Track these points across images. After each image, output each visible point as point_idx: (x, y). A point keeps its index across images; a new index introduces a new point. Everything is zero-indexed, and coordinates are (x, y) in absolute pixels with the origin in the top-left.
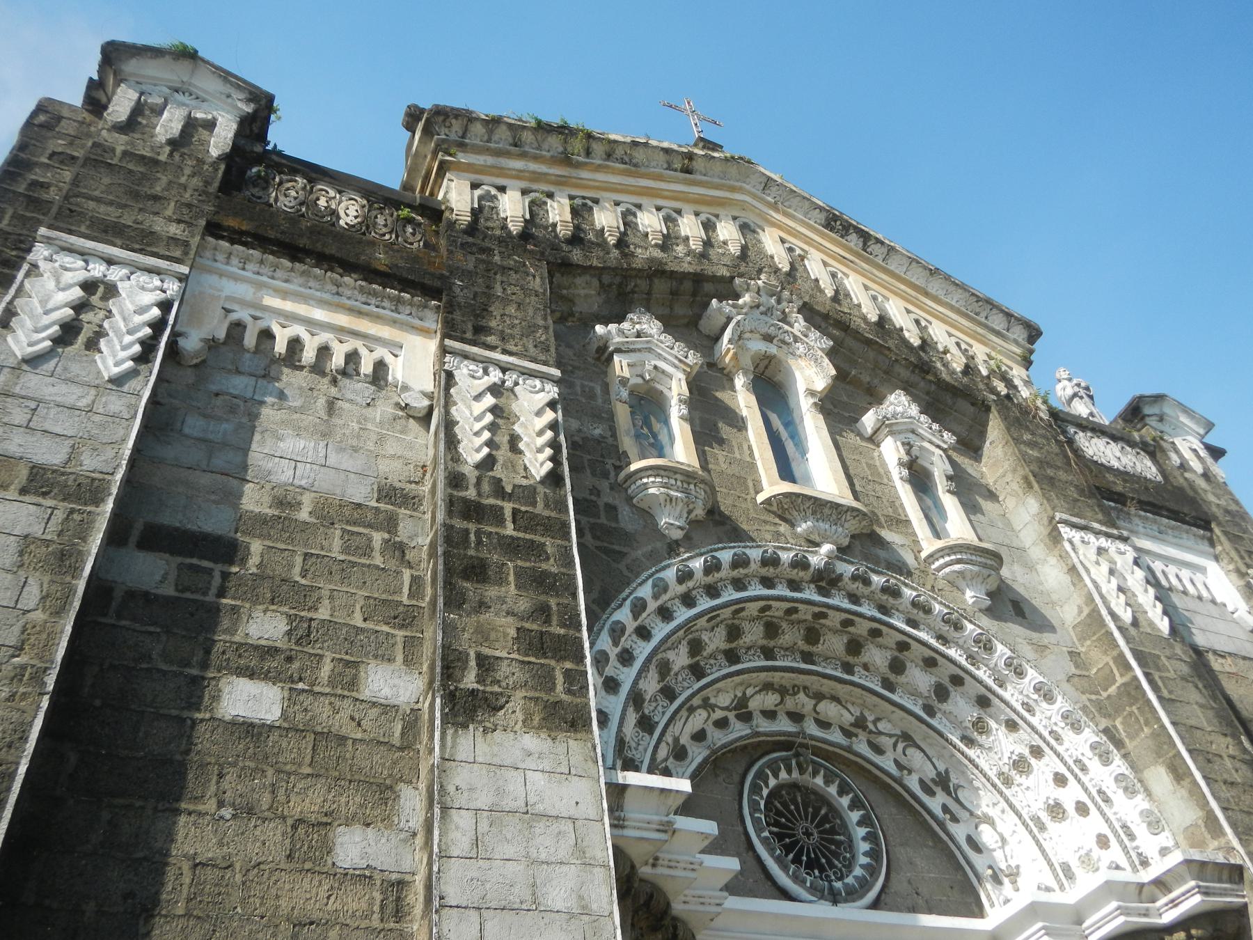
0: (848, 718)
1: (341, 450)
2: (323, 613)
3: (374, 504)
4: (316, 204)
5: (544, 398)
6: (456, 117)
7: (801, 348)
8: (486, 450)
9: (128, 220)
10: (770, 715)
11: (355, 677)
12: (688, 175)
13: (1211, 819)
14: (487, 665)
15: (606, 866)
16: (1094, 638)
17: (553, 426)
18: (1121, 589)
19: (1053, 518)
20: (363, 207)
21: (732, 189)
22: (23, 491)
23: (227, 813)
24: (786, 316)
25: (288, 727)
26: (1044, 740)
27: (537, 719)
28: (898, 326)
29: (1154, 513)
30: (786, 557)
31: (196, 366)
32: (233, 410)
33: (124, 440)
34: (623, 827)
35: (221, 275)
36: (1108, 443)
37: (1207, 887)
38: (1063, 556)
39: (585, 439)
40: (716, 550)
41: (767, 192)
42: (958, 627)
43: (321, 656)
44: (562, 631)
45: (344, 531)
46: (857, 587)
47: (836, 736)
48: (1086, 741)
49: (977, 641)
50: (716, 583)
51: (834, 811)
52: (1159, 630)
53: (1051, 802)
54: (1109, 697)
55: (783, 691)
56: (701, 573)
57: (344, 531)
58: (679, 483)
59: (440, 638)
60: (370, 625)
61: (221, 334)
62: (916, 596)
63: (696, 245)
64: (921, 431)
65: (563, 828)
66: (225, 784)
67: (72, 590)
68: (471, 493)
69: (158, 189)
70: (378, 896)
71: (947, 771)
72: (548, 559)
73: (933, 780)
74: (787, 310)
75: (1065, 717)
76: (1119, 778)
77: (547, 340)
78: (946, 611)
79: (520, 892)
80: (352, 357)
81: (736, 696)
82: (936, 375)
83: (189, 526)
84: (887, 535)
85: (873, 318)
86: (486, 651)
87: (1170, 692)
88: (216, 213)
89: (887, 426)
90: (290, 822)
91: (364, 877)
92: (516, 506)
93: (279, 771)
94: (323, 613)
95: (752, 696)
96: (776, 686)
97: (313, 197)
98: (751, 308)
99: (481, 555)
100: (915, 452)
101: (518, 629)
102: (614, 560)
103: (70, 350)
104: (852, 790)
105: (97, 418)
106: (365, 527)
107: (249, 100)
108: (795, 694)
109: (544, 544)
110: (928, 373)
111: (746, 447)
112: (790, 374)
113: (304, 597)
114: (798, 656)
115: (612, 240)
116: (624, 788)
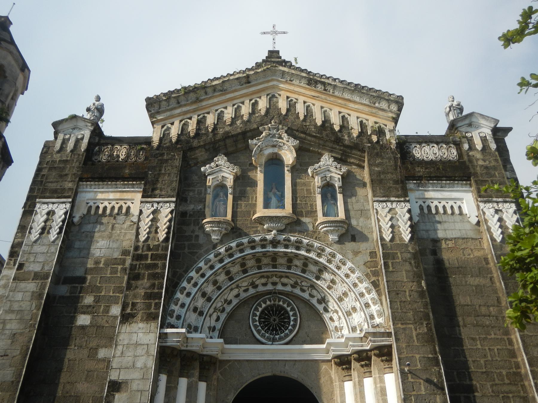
0: (292, 282)
1: (113, 241)
2: (103, 294)
3: (120, 257)
5: (169, 210)
6: (155, 103)
8: (147, 235)
9: (58, 187)
10: (265, 285)
11: (109, 310)
12: (249, 84)
14: (134, 305)
15: (154, 356)
17: (170, 221)
18: (392, 226)
20: (127, 150)
21: (268, 81)
22: (33, 280)
23: (76, 348)
25: (92, 325)
27: (145, 318)
29: (437, 180)
30: (257, 239)
31: (79, 225)
32: (87, 236)
33: (54, 259)
34: (167, 343)
35: (86, 192)
37: (374, 340)
40: (229, 243)
41: (284, 76)
42: (323, 250)
43: (101, 305)
44: (157, 291)
45: (111, 267)
47: (288, 289)
50: (233, 252)
51: (287, 312)
52: (405, 241)
55: (268, 277)
56: (225, 252)
57: (111, 267)
58: (216, 225)
59: (123, 300)
60: (114, 294)
61: (85, 212)
63: (245, 118)
64: (331, 169)
65: (144, 347)
66: (77, 341)
67: (42, 303)
68: (140, 252)
69: (67, 172)
70: (106, 364)
71: (324, 297)
75: (358, 278)
76: (372, 299)
78: (320, 245)
79: (131, 364)
80: (121, 208)
82: (342, 143)
83: (74, 275)
84: (305, 220)
85: (319, 123)
86: (135, 301)
88: (82, 173)
89: (315, 172)
90: (89, 348)
91: (103, 360)
93: (88, 337)
94: (103, 294)
96: (265, 276)
97: (113, 152)
99: (139, 272)
100: (328, 179)
101: (145, 293)
103: (44, 235)
104: (291, 304)
105: (49, 255)
106: (117, 265)
107: (92, 125)
108: (272, 278)
111: (255, 197)
113: (99, 289)
114: (271, 266)
115: (210, 130)
116: (167, 333)
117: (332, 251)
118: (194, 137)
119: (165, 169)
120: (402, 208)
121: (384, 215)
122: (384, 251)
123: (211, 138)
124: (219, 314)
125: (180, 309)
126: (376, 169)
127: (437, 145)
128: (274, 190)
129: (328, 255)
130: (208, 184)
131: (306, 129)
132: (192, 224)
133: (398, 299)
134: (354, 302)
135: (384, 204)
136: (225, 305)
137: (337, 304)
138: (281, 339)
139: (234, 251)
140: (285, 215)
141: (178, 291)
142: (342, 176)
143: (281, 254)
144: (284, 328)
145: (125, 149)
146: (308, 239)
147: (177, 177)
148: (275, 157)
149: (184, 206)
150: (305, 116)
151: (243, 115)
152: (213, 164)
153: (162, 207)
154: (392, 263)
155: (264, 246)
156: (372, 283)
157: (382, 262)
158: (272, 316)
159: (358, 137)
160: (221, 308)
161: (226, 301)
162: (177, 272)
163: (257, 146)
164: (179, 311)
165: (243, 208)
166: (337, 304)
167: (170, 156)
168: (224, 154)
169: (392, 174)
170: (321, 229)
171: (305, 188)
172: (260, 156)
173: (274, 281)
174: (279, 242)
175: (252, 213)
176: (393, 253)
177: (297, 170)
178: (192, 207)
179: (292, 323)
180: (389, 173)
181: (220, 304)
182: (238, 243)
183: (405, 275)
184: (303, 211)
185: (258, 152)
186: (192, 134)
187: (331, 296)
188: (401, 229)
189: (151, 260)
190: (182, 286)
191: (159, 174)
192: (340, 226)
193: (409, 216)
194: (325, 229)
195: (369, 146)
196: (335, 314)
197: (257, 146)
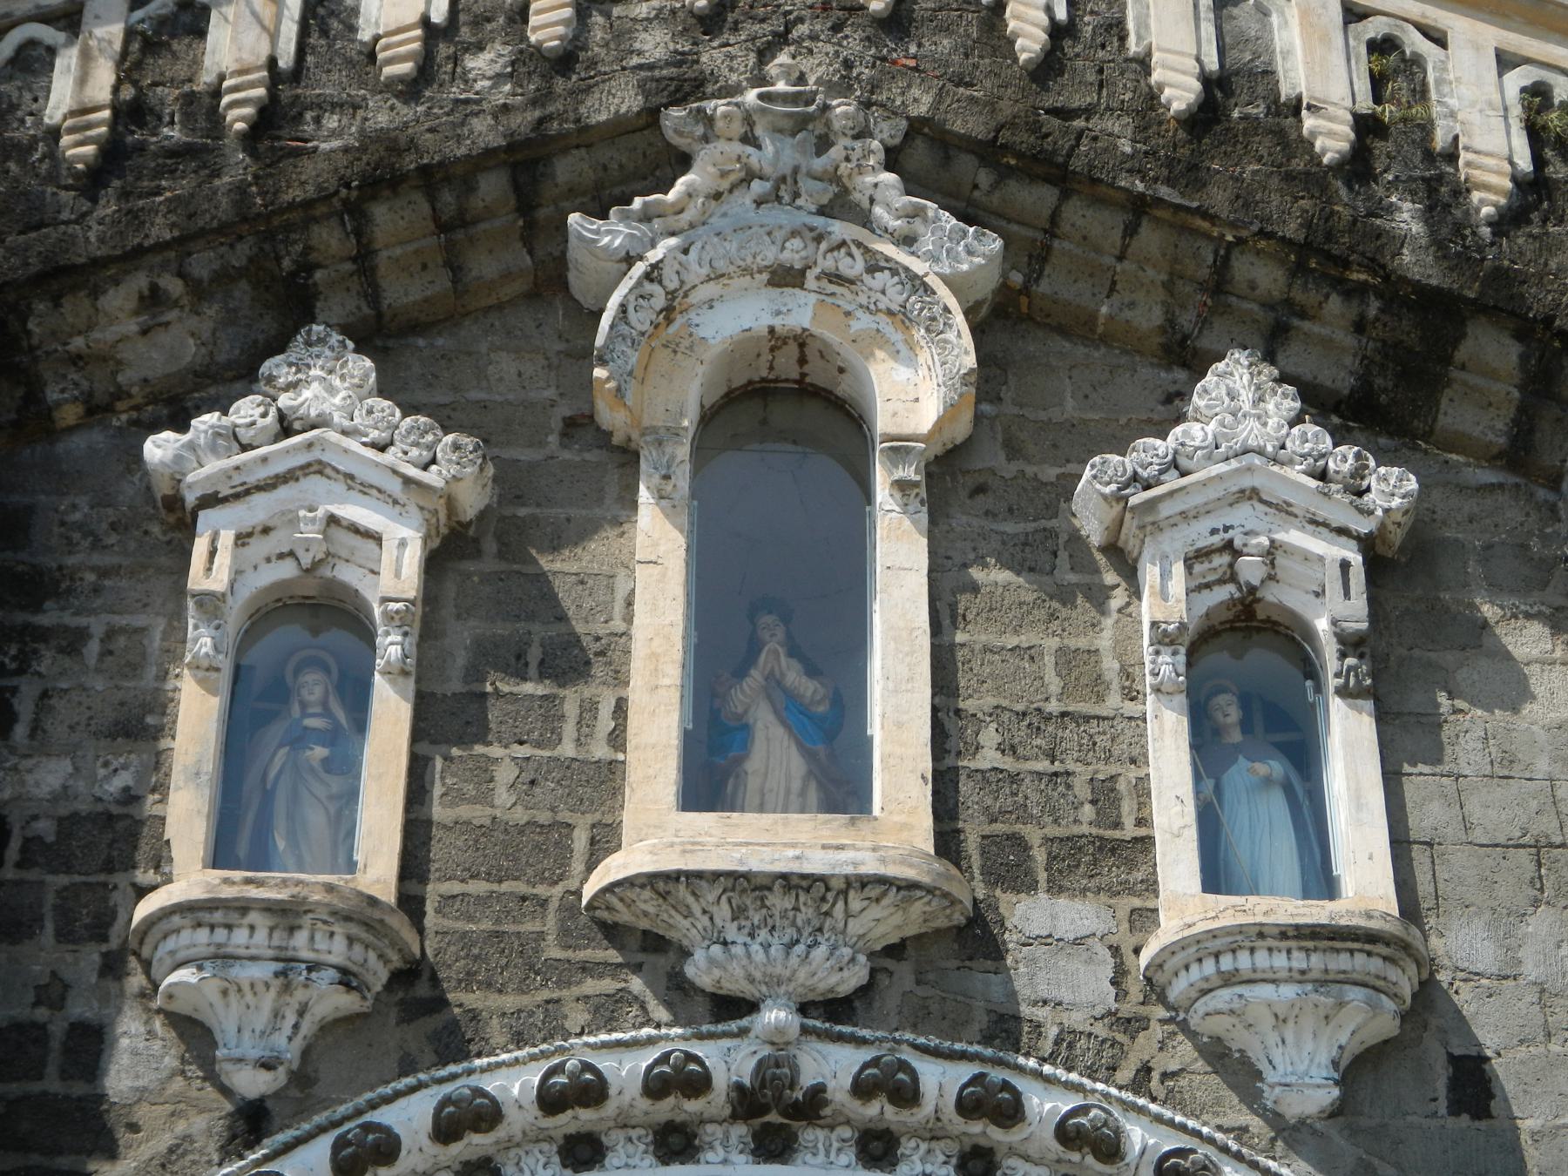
24: (845, 191)
39: (70, 824)
40: (373, 1106)
46: (877, 1110)
62: (1074, 1112)
74: (844, 168)
82: (1374, 265)
100: (1251, 568)
110: (1346, 265)
112: (864, 382)
115: (238, 119)
118: (94, 179)
123: (240, 189)
128: (774, 658)
130: (197, 579)
131: (1065, 144)
132: (49, 927)
140: (870, 867)
148: (787, 365)
150: (1058, 32)
152: (247, 410)
155: (675, 1140)
159: (1509, 220)
163: (639, 269)
165: (503, 797)
168: (346, 330)
171: (1052, 643)
172: (663, 356)
174: (812, 1106)
175: (580, 840)
177: (980, 490)
178: (49, 776)
182: (446, 1101)
184: (1033, 835)
185: (641, 320)
186: (79, 151)
192: (1346, 980)
197: (639, 269)
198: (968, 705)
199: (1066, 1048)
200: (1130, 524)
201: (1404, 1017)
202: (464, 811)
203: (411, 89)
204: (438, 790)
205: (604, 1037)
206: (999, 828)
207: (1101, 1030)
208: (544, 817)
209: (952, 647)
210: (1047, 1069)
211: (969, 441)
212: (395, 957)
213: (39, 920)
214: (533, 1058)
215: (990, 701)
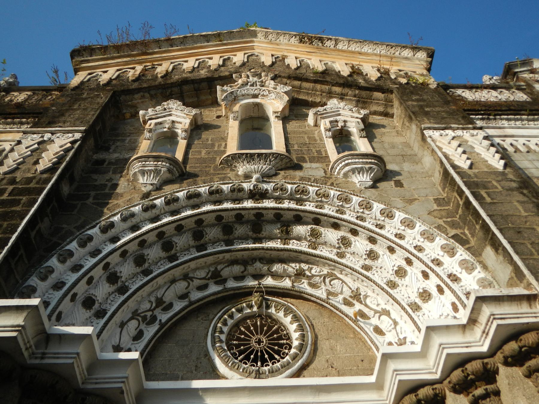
4: (4, 100)
6: (84, 50)
7: (273, 96)
13: (517, 269)
16: (448, 185)
17: (67, 151)
18: (464, 152)
19: (421, 129)
26: (411, 253)
28: (337, 71)
29: (515, 115)
30: (225, 188)
36: (489, 92)
38: (429, 147)
47: (287, 283)
48: (438, 246)
49: (360, 205)
53: (421, 291)
54: (460, 216)
72: (18, 205)
73: (351, 297)
74: (264, 80)
75: (423, 234)
76: (463, 263)
77: (91, 118)
78: (340, 193)
81: (210, 271)
87: (492, 199)
89: (319, 115)
92: (17, 186)
95: (222, 269)
98: (242, 85)
102: (101, 207)
108: (253, 263)
109: (22, 199)
115: (159, 76)
117: (364, 199)
118: (134, 81)
119: (80, 105)
120: (473, 136)
121: (446, 143)
122: (465, 180)
123: (160, 82)
124: (143, 327)
125: (51, 291)
126: (416, 103)
127: (495, 90)
129: (357, 207)
132: (111, 172)
133: (524, 240)
134: (421, 282)
135: (442, 132)
136: (157, 312)
137: (387, 293)
138: (273, 373)
139: (183, 207)
141: (55, 256)
142: (361, 119)
143: (270, 215)
144: (279, 355)
145: (25, 95)
146: (317, 187)
147: (96, 111)
149: (102, 154)
151: (210, 66)
152: (158, 108)
153: (58, 137)
154: (486, 192)
156: (453, 237)
157: (467, 192)
158: (254, 335)
160: (149, 314)
161: (160, 302)
162: (63, 228)
164: (47, 295)
166: (387, 293)
167: (92, 95)
169: (442, 107)
170: (339, 173)
173: (258, 272)
176: (482, 181)
178: (116, 155)
179: (296, 343)
180: (436, 107)
181: (146, 306)
183: (520, 208)
184: (306, 156)
187: (371, 280)
188: (483, 156)
189: (8, 196)
190: (68, 247)
191: (67, 110)
193: (490, 142)
194: (347, 169)
195: (397, 88)
196: (384, 317)
198: (292, 143)
199: (316, 181)
200: (319, 117)
201: (383, 175)
202: (195, 157)
203: (190, 72)
204: (190, 154)
205: (222, 182)
206: (299, 156)
207: (323, 179)
208: (211, 157)
209: (288, 137)
210: (312, 184)
211: (288, 116)
212: (180, 171)
213: (109, 171)
214: (208, 186)
215: (295, 142)
